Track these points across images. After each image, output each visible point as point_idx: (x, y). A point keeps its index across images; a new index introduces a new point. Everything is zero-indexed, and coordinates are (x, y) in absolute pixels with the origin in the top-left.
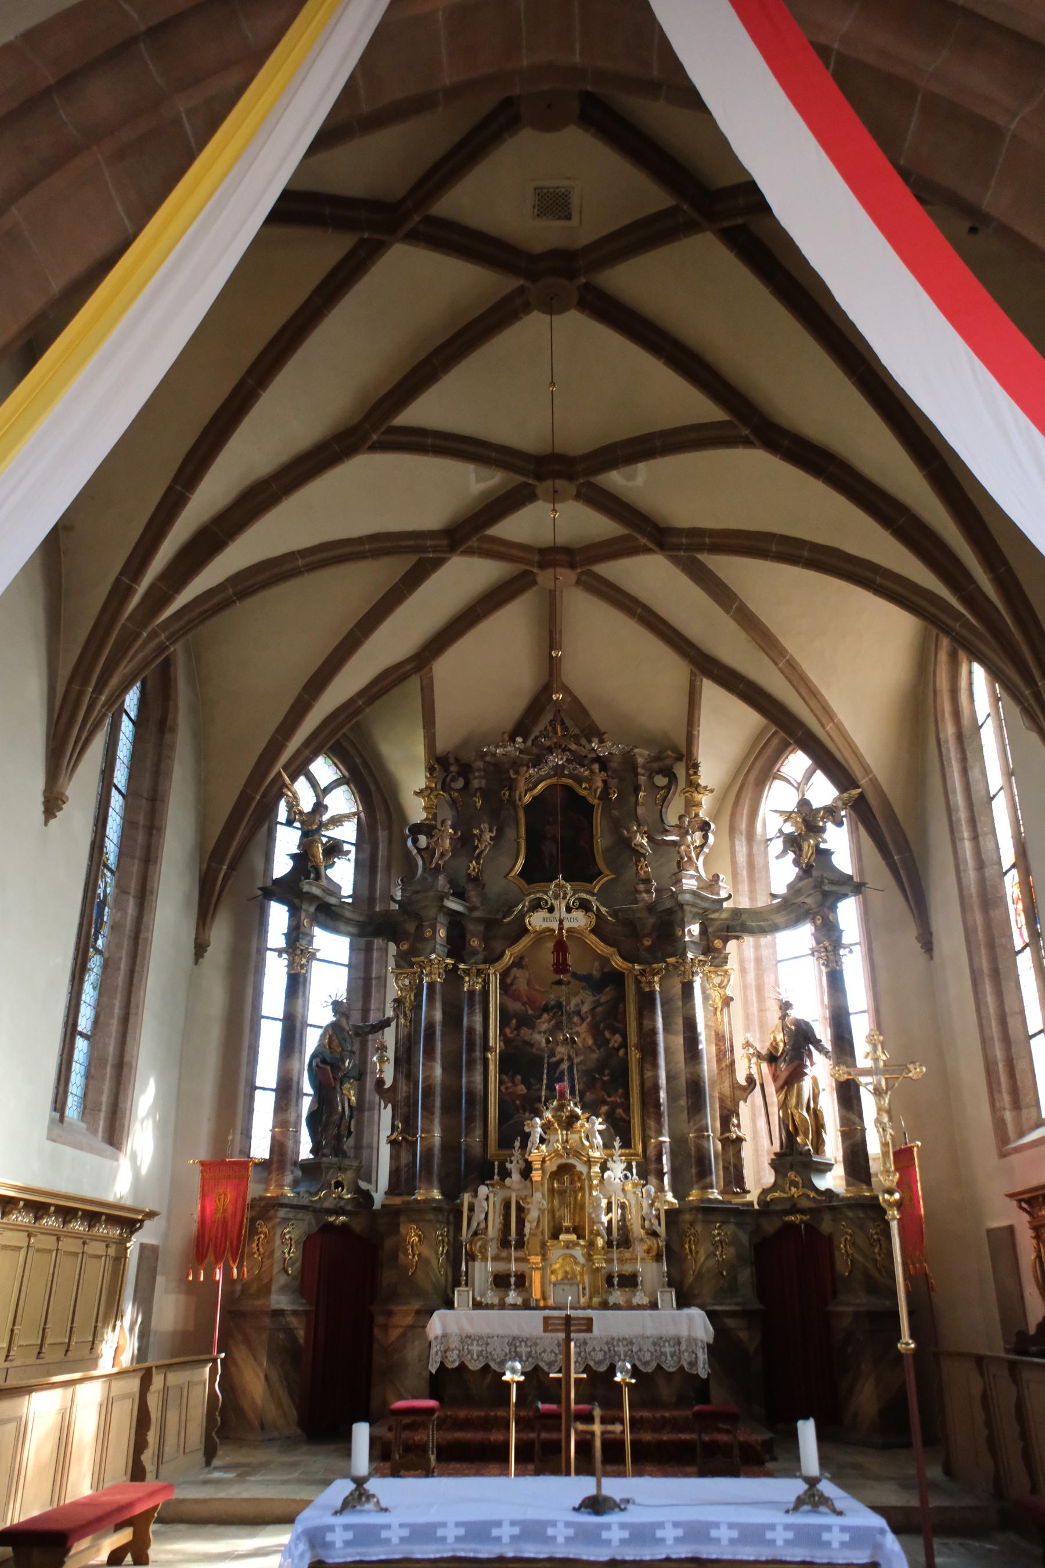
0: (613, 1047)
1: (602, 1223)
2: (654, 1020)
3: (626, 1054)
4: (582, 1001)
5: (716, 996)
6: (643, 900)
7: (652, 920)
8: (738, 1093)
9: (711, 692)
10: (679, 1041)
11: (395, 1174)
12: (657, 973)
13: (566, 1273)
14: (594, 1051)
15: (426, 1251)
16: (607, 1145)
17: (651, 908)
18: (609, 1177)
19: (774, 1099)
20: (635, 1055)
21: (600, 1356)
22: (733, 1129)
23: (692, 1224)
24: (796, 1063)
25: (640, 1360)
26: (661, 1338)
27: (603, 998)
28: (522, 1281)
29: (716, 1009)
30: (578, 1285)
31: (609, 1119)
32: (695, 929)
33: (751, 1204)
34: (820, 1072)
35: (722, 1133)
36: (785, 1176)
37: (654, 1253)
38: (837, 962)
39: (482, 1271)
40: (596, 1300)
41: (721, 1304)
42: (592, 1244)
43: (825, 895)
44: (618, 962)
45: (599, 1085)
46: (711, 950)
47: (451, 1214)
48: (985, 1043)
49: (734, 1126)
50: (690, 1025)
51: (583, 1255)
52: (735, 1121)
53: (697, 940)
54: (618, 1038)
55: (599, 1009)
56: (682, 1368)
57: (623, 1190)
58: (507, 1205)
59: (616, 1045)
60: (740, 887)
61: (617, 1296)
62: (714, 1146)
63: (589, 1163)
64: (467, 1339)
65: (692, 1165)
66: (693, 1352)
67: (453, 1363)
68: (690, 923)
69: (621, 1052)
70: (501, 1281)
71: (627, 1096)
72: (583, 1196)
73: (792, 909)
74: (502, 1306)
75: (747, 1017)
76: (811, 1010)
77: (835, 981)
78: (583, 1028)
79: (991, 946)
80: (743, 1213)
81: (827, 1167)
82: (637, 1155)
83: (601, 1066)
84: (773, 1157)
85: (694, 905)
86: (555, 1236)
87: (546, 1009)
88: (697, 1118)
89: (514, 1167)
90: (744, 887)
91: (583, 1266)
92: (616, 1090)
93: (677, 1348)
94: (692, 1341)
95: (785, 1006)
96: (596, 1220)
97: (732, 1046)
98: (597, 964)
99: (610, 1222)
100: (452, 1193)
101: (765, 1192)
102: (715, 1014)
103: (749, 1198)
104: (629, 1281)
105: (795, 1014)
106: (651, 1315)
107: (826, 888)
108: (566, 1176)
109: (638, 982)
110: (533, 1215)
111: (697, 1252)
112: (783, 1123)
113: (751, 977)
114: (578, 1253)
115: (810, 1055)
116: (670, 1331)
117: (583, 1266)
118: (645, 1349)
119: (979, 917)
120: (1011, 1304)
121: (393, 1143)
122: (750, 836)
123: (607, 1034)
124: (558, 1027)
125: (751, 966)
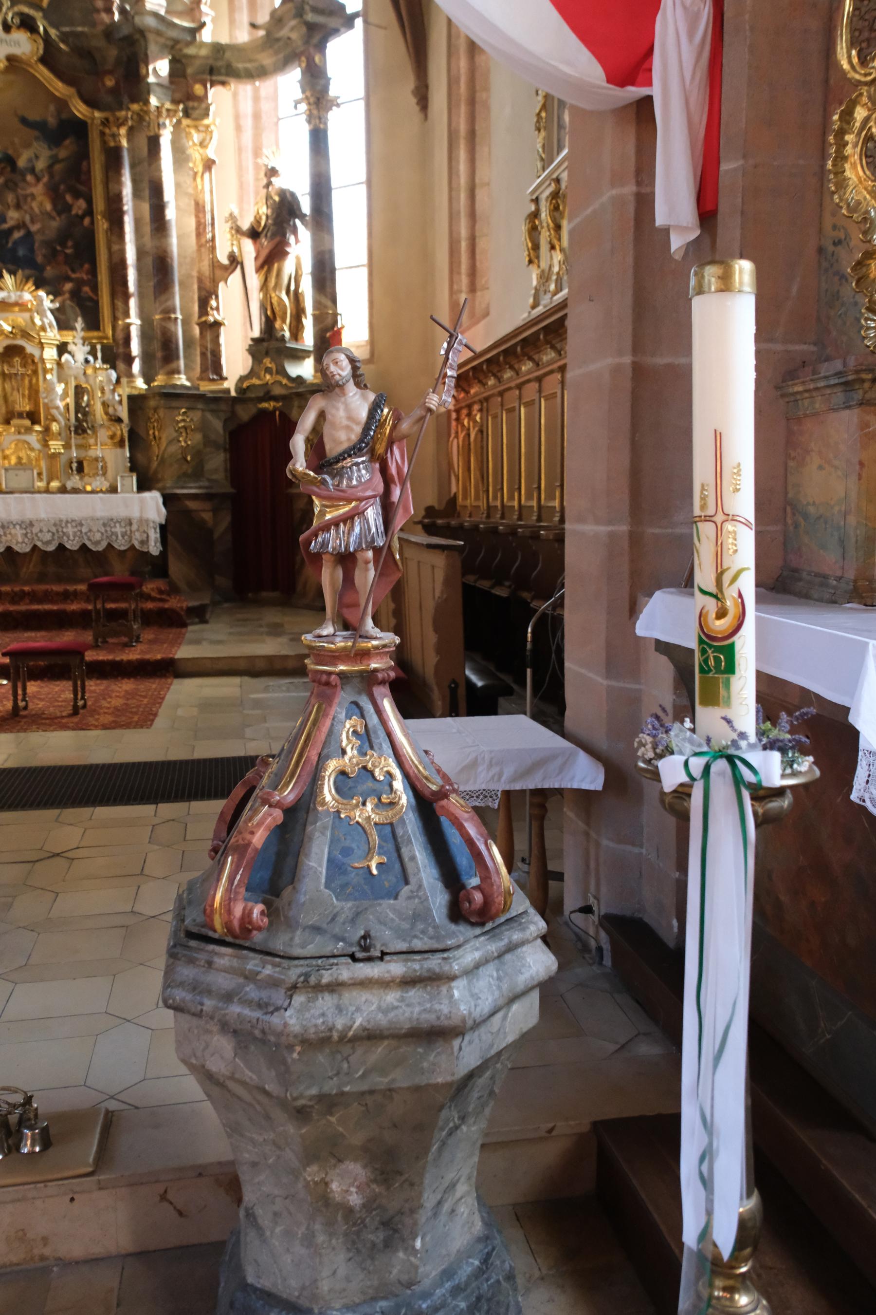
0: (77, 215)
1: (57, 408)
2: (119, 183)
3: (92, 223)
4: (35, 155)
5: (196, 155)
6: (102, 22)
7: (113, 53)
8: (218, 273)
12: (122, 124)
13: (19, 459)
14: (54, 219)
16: (63, 325)
18: (67, 361)
20: (102, 225)
21: (48, 537)
22: (210, 312)
23: (155, 410)
24: (278, 239)
25: (89, 540)
26: (112, 520)
27: (63, 153)
29: (196, 174)
30: (33, 470)
31: (75, 295)
33: (228, 391)
34: (300, 248)
35: (200, 317)
36: (261, 362)
37: (117, 439)
38: (320, 118)
40: (55, 484)
41: (183, 488)
42: (47, 430)
43: (312, 28)
45: (61, 258)
49: (212, 309)
51: (38, 440)
52: (213, 303)
53: (166, 82)
54: (82, 204)
55: (58, 167)
56: (133, 547)
57: (85, 373)
59: (80, 212)
60: (237, 16)
61: (74, 481)
65: (162, 350)
66: (144, 532)
68: (156, 59)
69: (87, 221)
71: (94, 272)
72: (37, 380)
75: (241, 186)
77: (319, 140)
78: (38, 190)
79: (472, 102)
80: (218, 400)
82: (107, 338)
83: (63, 237)
84: (251, 343)
85: (158, 33)
88: (163, 298)
91: (40, 451)
92: (82, 266)
93: (128, 528)
94: (143, 521)
95: (272, 172)
96: (50, 405)
97: (213, 219)
98: (52, 108)
99: (67, 407)
101: (242, 379)
102: (195, 179)
103: (226, 385)
105: (278, 183)
106: (101, 498)
107: (310, 17)
109: (103, 134)
111: (160, 438)
112: (263, 307)
114: (33, 439)
115: (295, 231)
116: (121, 512)
117: (40, 451)
118: (95, 529)
119: (463, 63)
123: (69, 198)
125: (248, 123)
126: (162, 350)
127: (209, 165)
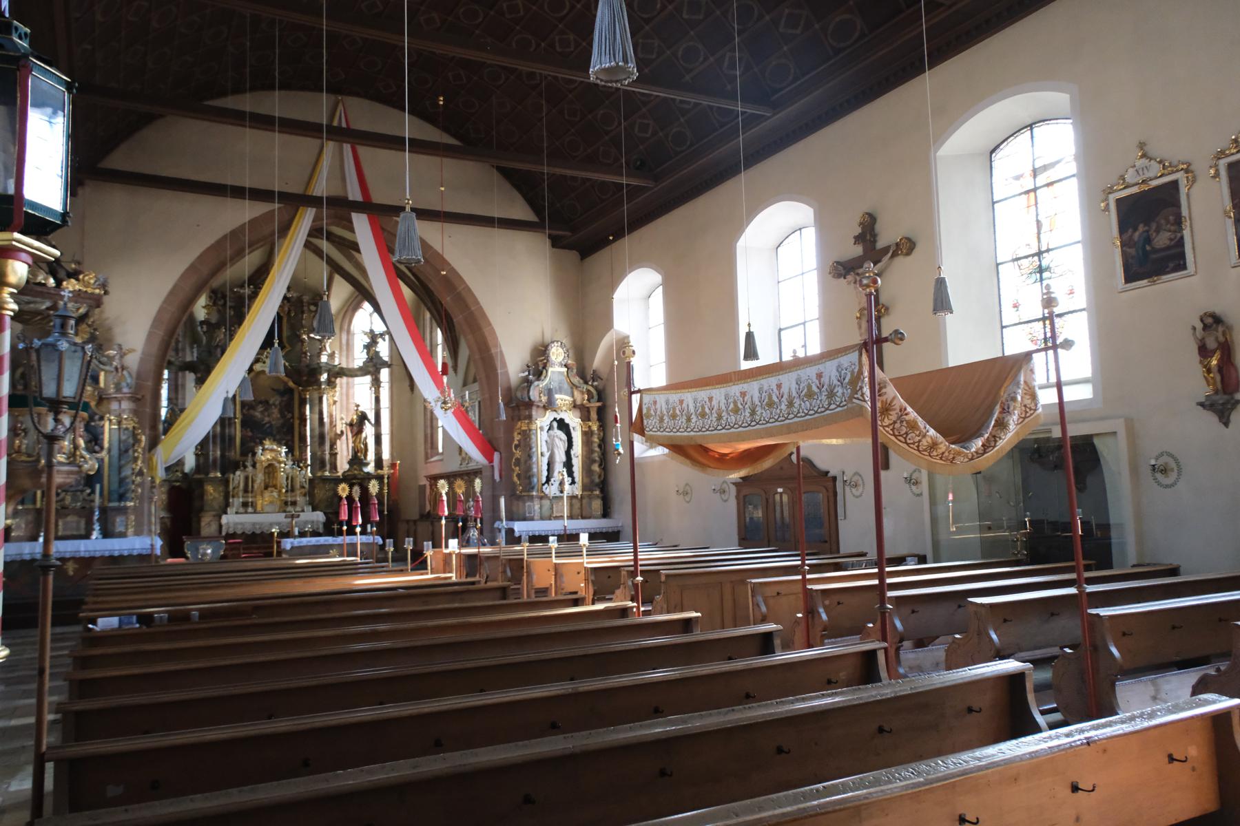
4: (275, 400)
9: (338, 279)
10: (317, 416)
11: (198, 465)
15: (216, 495)
17: (307, 366)
19: (350, 441)
20: (297, 422)
28: (253, 505)
32: (324, 377)
34: (369, 431)
39: (237, 502)
44: (291, 384)
46: (331, 383)
47: (226, 482)
48: (425, 427)
50: (321, 413)
58: (247, 478)
62: (327, 457)
63: (280, 462)
64: (236, 524)
67: (231, 531)
70: (245, 505)
73: (363, 371)
74: (246, 512)
76: (368, 408)
77: (377, 400)
81: (367, 464)
86: (266, 488)
87: (261, 402)
89: (249, 464)
90: (344, 359)
100: (223, 473)
104: (294, 503)
108: (271, 469)
110: (258, 481)
113: (344, 390)
114: (275, 494)
120: (422, 506)
121: (196, 455)
122: (348, 332)
124: (266, 410)
126: (319, 463)
127: (335, 402)
